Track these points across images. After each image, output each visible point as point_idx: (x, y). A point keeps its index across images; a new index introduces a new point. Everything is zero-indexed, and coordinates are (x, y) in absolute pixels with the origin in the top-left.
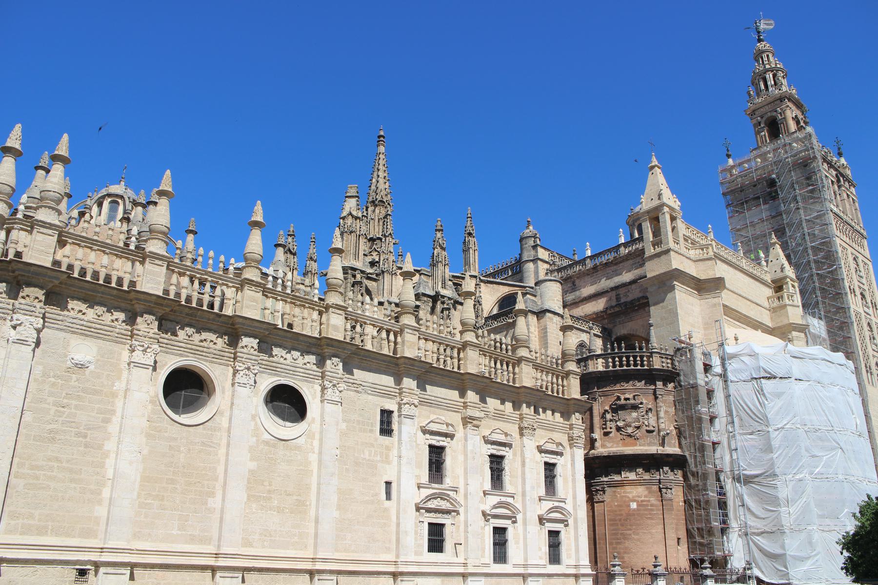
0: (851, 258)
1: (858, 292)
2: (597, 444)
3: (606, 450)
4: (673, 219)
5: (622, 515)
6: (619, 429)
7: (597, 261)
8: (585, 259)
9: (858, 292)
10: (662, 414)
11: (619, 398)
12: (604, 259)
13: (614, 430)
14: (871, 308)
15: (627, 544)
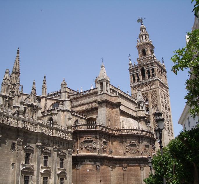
0: (163, 95)
1: (164, 106)
2: (79, 152)
3: (81, 154)
4: (107, 84)
5: (84, 173)
6: (85, 148)
7: (84, 94)
8: (80, 93)
9: (164, 106)
10: (98, 144)
11: (86, 138)
12: (86, 93)
13: (84, 148)
14: (168, 110)
15: (86, 182)
